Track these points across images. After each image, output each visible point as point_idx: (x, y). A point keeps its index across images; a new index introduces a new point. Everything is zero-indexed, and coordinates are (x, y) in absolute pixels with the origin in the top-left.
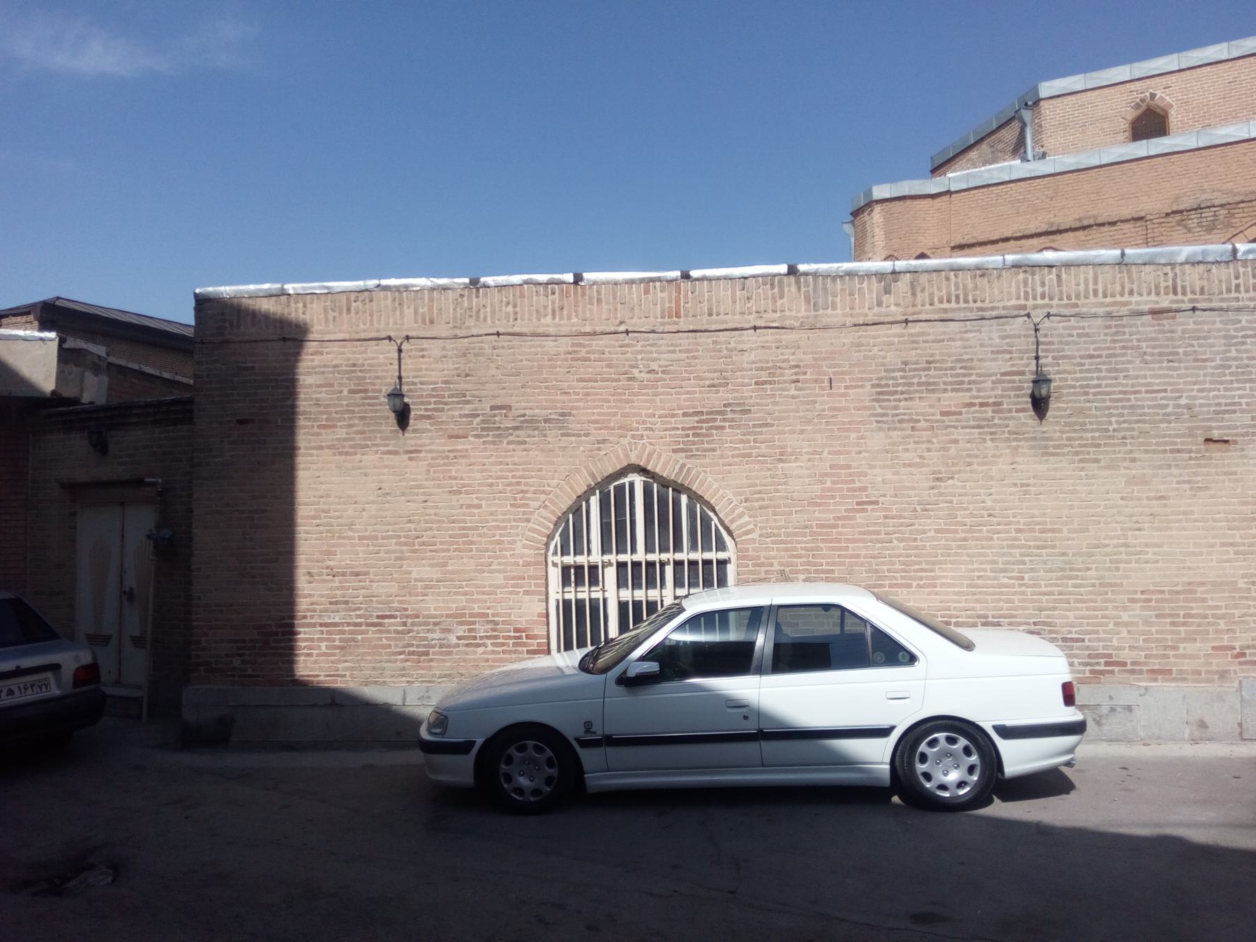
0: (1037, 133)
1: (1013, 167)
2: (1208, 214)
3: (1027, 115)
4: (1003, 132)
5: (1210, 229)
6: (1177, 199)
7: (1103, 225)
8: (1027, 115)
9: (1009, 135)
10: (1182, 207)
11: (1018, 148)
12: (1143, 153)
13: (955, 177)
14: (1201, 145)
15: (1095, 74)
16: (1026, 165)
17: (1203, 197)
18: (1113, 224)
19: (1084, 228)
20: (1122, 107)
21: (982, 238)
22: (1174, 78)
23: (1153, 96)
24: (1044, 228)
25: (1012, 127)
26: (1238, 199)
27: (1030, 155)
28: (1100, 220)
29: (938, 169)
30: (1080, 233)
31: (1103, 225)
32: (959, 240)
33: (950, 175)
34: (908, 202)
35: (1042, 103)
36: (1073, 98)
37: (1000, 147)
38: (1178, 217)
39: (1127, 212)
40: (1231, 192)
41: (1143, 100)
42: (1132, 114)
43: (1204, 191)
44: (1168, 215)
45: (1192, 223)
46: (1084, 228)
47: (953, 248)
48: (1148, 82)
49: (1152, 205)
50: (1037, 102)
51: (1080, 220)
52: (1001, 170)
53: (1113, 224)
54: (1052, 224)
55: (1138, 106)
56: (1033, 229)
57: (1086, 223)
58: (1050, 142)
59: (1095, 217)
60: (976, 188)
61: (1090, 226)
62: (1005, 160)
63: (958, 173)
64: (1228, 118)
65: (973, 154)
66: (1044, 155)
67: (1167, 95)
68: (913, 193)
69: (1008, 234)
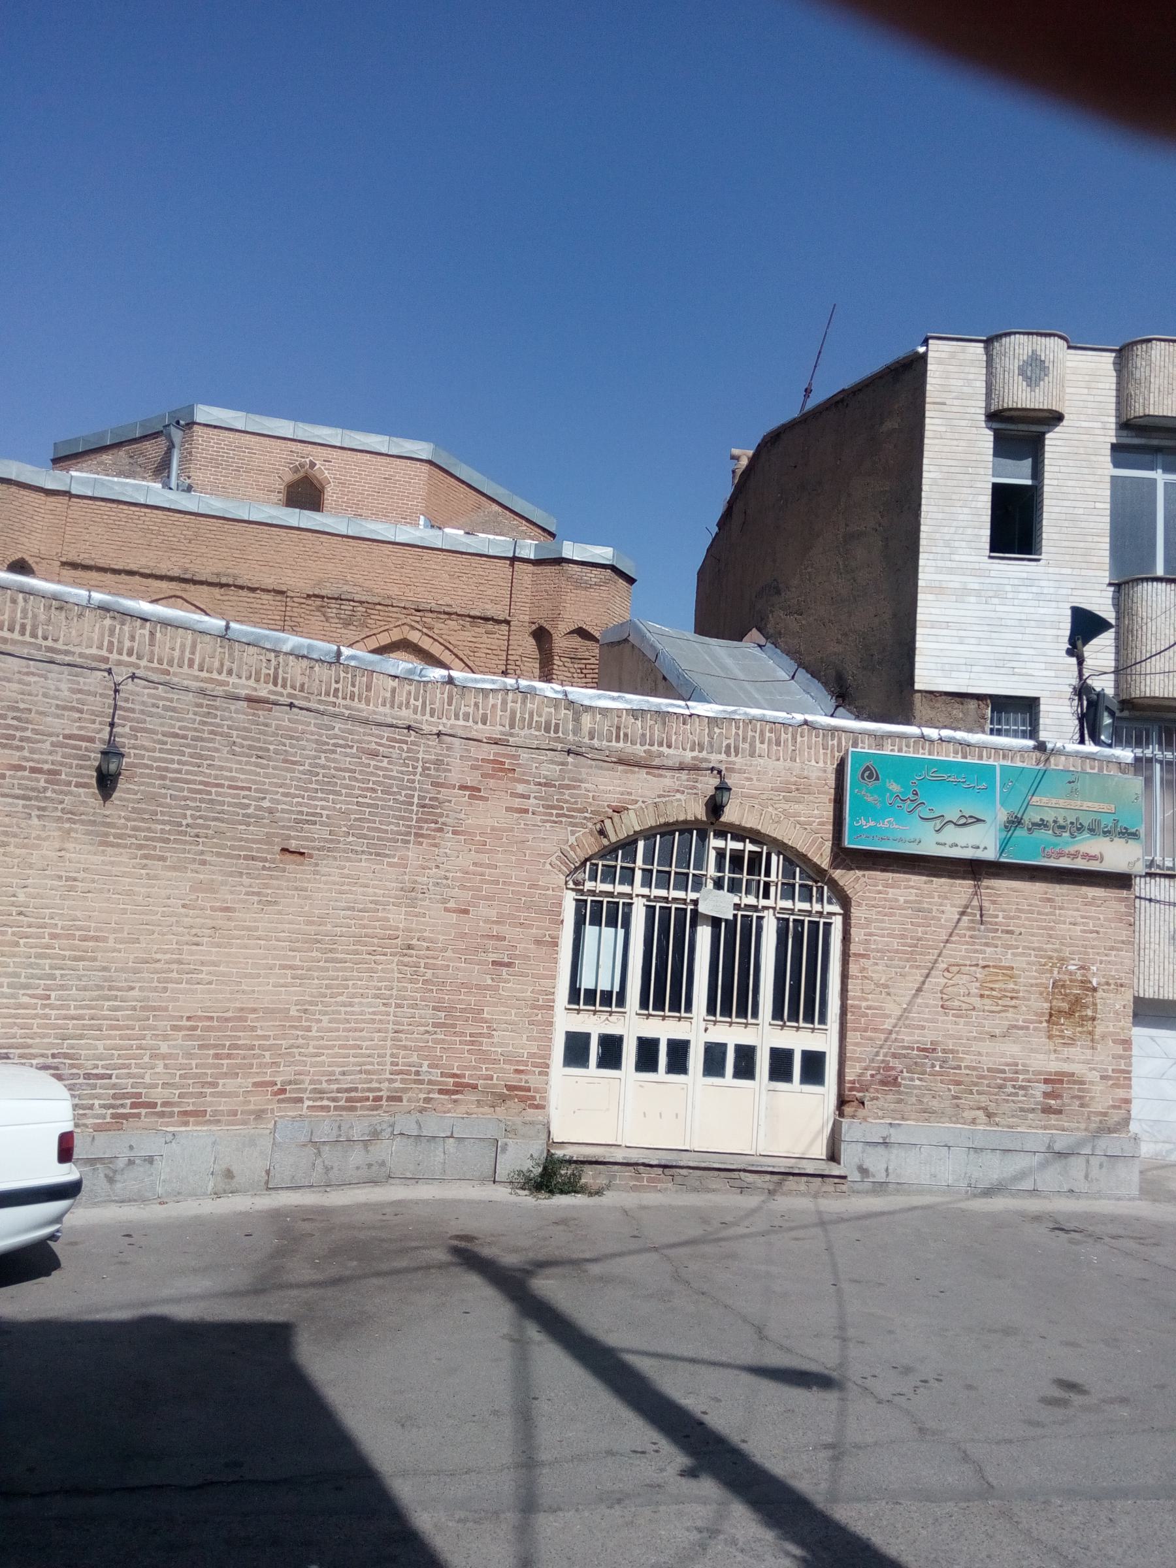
0: (186, 459)
1: (151, 490)
2: (347, 606)
3: (177, 435)
4: (147, 445)
5: (347, 624)
6: (320, 583)
7: (242, 588)
8: (177, 435)
9: (153, 450)
10: (323, 593)
11: (162, 470)
12: (294, 523)
13: (79, 478)
14: (351, 533)
15: (257, 418)
16: (166, 492)
17: (345, 588)
18: (253, 590)
19: (222, 585)
20: (278, 467)
21: (102, 563)
22: (336, 453)
23: (313, 465)
24: (176, 572)
25: (157, 442)
26: (376, 600)
27: (173, 484)
28: (240, 582)
29: (61, 460)
30: (216, 591)
31: (242, 588)
32: (72, 557)
33: (74, 473)
34: (14, 489)
35: (196, 428)
36: (231, 435)
37: (141, 460)
38: (318, 602)
39: (269, 582)
40: (369, 591)
41: (302, 465)
42: (289, 477)
43: (346, 582)
44: (309, 596)
45: (332, 613)
46: (222, 585)
47: (64, 564)
48: (310, 448)
49: (296, 581)
50: (191, 424)
51: (218, 575)
52: (137, 488)
53: (253, 590)
54: (186, 570)
55: (296, 470)
56: (164, 568)
57: (224, 580)
58: (198, 476)
59: (235, 577)
60: (103, 500)
61: (228, 585)
62: (144, 478)
63: (84, 475)
64: (381, 515)
65: (107, 458)
66: (189, 489)
67: (327, 470)
68: (22, 479)
69: (134, 567)
